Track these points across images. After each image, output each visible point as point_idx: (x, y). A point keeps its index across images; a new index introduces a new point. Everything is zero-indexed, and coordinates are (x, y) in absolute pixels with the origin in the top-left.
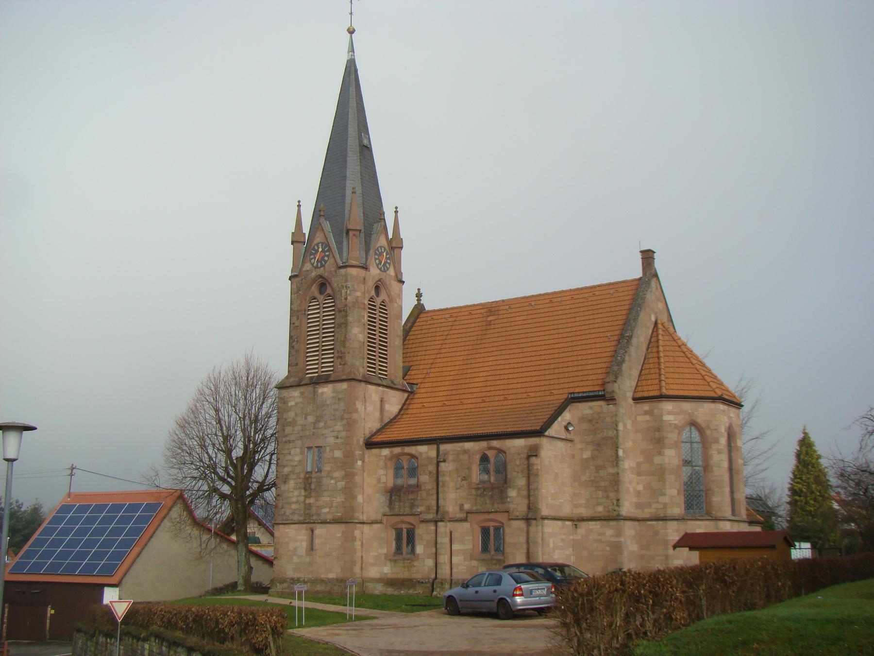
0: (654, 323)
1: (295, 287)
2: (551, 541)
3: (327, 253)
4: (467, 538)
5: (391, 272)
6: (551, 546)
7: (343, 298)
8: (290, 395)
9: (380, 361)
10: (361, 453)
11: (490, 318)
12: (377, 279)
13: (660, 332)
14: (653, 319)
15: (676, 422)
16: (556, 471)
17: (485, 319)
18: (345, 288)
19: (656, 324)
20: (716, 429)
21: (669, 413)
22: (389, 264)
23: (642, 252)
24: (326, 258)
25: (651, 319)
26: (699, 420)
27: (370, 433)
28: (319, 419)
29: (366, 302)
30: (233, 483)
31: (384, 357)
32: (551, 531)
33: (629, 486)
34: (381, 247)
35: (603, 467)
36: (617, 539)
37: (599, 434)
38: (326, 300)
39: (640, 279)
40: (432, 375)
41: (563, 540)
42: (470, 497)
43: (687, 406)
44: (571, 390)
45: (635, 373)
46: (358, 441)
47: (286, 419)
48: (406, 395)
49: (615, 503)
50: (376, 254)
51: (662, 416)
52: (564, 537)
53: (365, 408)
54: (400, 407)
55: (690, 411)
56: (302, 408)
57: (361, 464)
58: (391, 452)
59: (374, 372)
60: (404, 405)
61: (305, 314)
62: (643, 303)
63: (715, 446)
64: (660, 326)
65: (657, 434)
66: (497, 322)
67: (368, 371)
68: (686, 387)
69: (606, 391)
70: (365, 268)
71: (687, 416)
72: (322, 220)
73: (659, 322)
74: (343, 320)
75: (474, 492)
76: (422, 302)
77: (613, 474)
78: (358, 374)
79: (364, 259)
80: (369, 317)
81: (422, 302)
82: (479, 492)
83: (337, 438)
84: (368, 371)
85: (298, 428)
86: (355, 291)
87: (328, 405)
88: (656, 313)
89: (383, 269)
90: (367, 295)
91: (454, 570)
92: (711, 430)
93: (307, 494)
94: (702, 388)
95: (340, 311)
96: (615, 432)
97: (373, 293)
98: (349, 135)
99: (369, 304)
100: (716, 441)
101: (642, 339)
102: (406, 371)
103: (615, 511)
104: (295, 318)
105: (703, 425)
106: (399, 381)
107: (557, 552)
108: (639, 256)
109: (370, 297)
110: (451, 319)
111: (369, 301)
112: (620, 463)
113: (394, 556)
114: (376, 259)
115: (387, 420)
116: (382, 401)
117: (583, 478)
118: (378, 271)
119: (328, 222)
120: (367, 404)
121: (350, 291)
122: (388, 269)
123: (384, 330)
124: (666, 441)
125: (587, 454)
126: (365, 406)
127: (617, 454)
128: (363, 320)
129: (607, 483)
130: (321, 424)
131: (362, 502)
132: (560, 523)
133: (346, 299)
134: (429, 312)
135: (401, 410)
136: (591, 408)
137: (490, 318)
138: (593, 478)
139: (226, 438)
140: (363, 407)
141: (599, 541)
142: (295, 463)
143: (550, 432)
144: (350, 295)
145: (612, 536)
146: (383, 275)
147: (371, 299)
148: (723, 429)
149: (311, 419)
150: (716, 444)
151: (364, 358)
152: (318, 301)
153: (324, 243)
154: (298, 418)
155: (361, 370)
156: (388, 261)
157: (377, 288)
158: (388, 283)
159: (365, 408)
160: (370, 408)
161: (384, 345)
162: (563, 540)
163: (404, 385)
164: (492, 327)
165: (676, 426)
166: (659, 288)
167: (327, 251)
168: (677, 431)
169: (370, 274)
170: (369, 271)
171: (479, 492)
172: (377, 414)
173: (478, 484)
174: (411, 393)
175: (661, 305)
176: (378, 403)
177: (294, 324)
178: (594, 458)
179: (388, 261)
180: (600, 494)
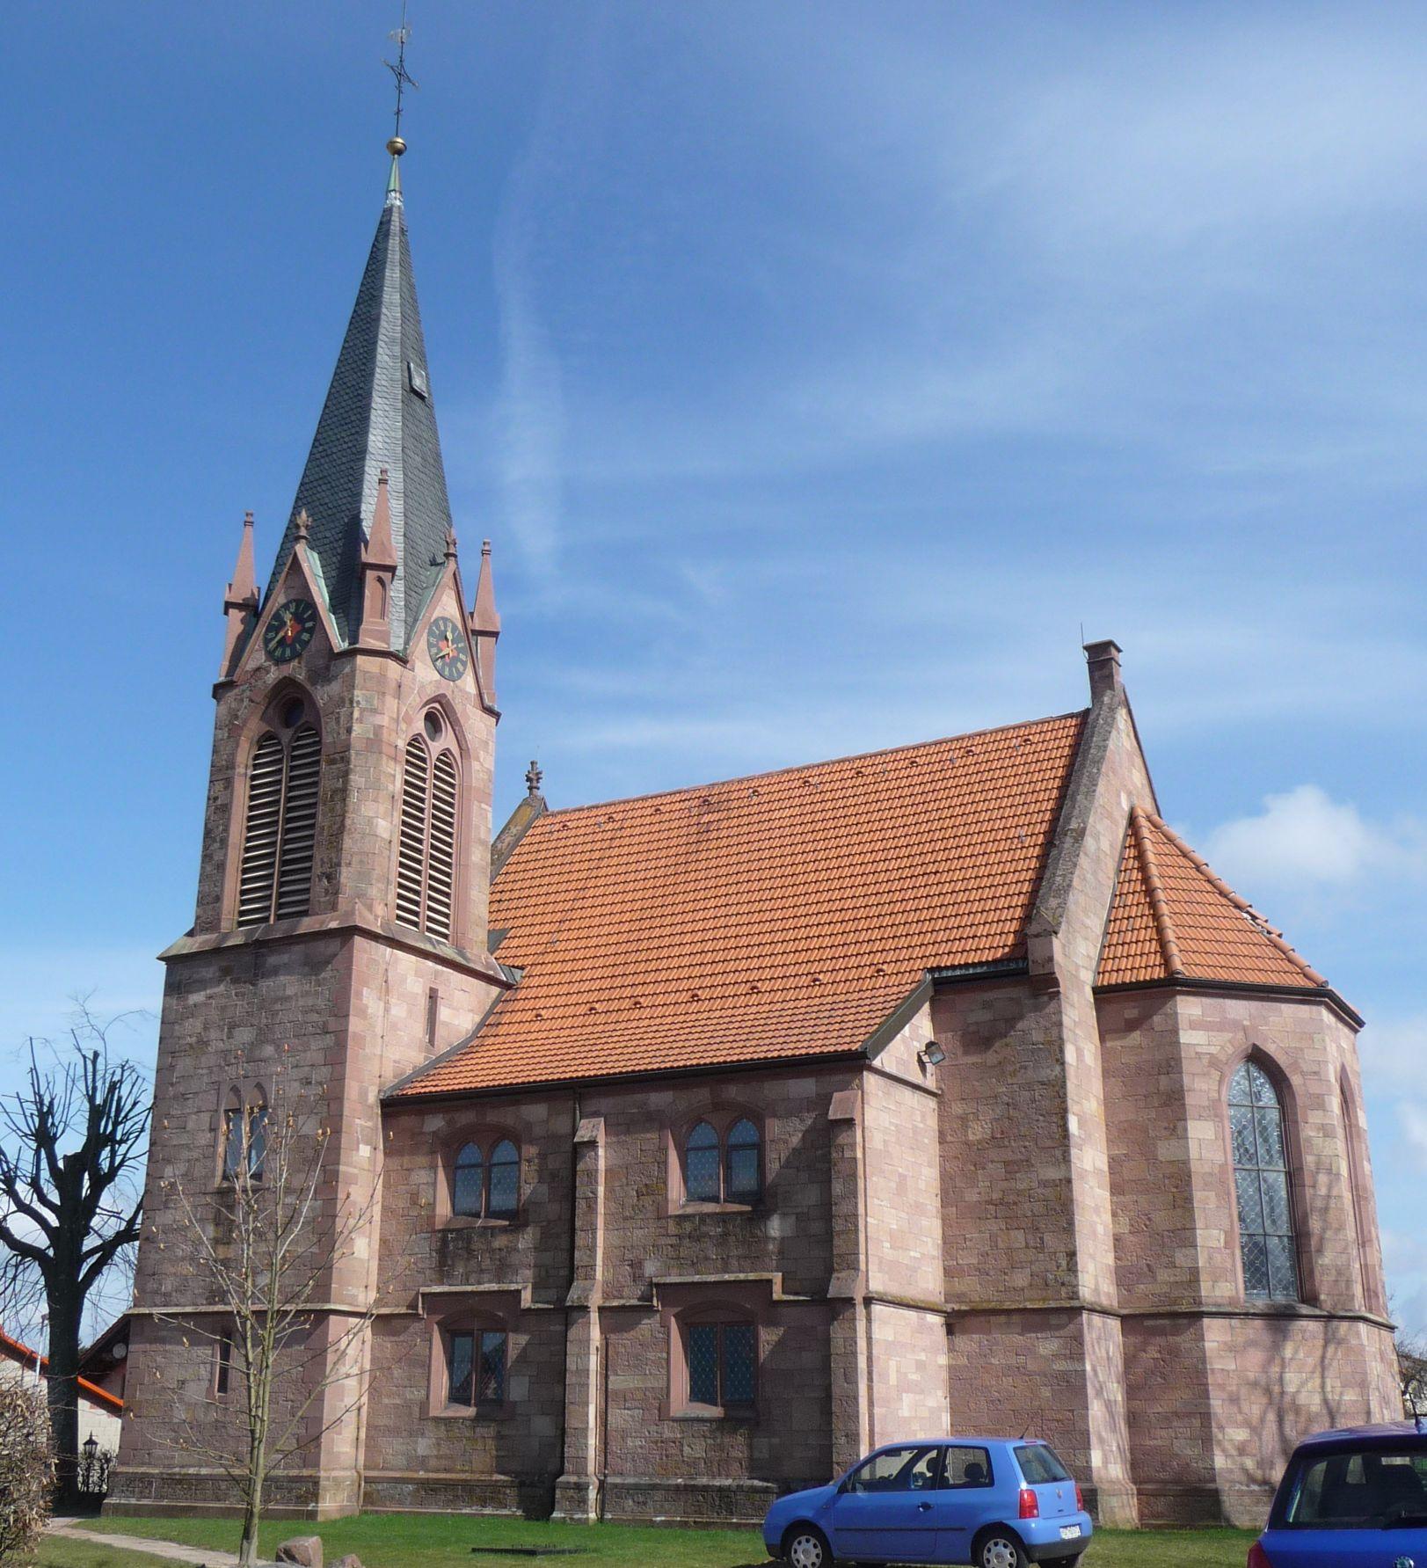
1: (223, 709)
2: (892, 1364)
3: (309, 624)
4: (651, 1355)
5: (468, 683)
6: (893, 1380)
9: (430, 909)
11: (706, 819)
12: (431, 692)
13: (1145, 832)
14: (1126, 807)
15: (1213, 1050)
17: (694, 820)
18: (347, 705)
19: (1132, 821)
21: (1194, 1026)
22: (464, 664)
23: (1086, 648)
24: (305, 636)
25: (1119, 803)
26: (1271, 1048)
27: (395, 1077)
28: (263, 1036)
29: (402, 744)
30: (53, 1220)
31: (442, 889)
33: (1095, 1218)
34: (445, 620)
38: (299, 739)
39: (1087, 712)
41: (920, 1366)
42: (663, 1241)
43: (1238, 1009)
44: (932, 962)
45: (1096, 924)
46: (363, 1094)
48: (495, 991)
49: (1064, 1263)
50: (431, 633)
51: (1175, 1032)
52: (923, 1357)
53: (387, 1010)
54: (478, 1019)
55: (1246, 1023)
56: (223, 1009)
58: (450, 1123)
59: (415, 924)
60: (490, 1013)
61: (246, 774)
62: (1103, 758)
63: (1315, 1117)
64: (1143, 822)
66: (725, 824)
67: (399, 918)
68: (1234, 962)
70: (402, 659)
71: (1240, 1035)
72: (301, 549)
73: (1140, 812)
74: (340, 784)
75: (672, 1228)
79: (402, 641)
80: (407, 783)
81: (538, 793)
82: (688, 1227)
84: (399, 918)
85: (210, 1060)
86: (374, 711)
87: (288, 999)
88: (1129, 794)
89: (447, 673)
90: (403, 726)
91: (614, 1447)
93: (220, 1235)
94: (1272, 965)
95: (332, 762)
96: (1058, 1068)
97: (419, 726)
98: (378, 363)
99: (409, 753)
100: (1319, 1103)
101: (1105, 845)
102: (496, 939)
103: (1063, 1284)
104: (219, 786)
106: (479, 956)
108: (1083, 657)
111: (410, 744)
112: (1074, 1152)
113: (446, 1408)
114: (430, 645)
115: (442, 1047)
116: (433, 996)
117: (972, 1196)
118: (437, 676)
119: (316, 555)
120: (393, 1001)
121: (362, 711)
122: (460, 675)
123: (444, 822)
124: (1190, 1100)
125: (977, 1132)
126: (387, 1003)
128: (391, 787)
129: (1038, 1208)
130: (269, 1050)
132: (912, 1315)
133: (349, 731)
134: (554, 815)
135: (482, 1024)
136: (987, 1005)
137: (706, 819)
139: (45, 1113)
140: (382, 1004)
141: (1020, 1370)
142: (195, 1155)
143: (885, 1060)
144: (360, 720)
146: (447, 688)
147: (415, 741)
148: (1332, 1075)
149: (245, 1035)
150: (1320, 1113)
152: (279, 743)
153: (302, 601)
154: (213, 1034)
155: (380, 910)
156: (461, 656)
157: (432, 720)
158: (458, 708)
159: (387, 1010)
160: (398, 1011)
161: (444, 859)
162: (920, 1366)
163: (488, 966)
165: (1214, 1062)
168: (1216, 1075)
169: (414, 678)
170: (413, 670)
171: (688, 1227)
172: (419, 1029)
173: (684, 1206)
174: (507, 986)
175: (1138, 778)
176: (423, 1003)
177: (216, 799)
179: (461, 656)
180: (1019, 1238)
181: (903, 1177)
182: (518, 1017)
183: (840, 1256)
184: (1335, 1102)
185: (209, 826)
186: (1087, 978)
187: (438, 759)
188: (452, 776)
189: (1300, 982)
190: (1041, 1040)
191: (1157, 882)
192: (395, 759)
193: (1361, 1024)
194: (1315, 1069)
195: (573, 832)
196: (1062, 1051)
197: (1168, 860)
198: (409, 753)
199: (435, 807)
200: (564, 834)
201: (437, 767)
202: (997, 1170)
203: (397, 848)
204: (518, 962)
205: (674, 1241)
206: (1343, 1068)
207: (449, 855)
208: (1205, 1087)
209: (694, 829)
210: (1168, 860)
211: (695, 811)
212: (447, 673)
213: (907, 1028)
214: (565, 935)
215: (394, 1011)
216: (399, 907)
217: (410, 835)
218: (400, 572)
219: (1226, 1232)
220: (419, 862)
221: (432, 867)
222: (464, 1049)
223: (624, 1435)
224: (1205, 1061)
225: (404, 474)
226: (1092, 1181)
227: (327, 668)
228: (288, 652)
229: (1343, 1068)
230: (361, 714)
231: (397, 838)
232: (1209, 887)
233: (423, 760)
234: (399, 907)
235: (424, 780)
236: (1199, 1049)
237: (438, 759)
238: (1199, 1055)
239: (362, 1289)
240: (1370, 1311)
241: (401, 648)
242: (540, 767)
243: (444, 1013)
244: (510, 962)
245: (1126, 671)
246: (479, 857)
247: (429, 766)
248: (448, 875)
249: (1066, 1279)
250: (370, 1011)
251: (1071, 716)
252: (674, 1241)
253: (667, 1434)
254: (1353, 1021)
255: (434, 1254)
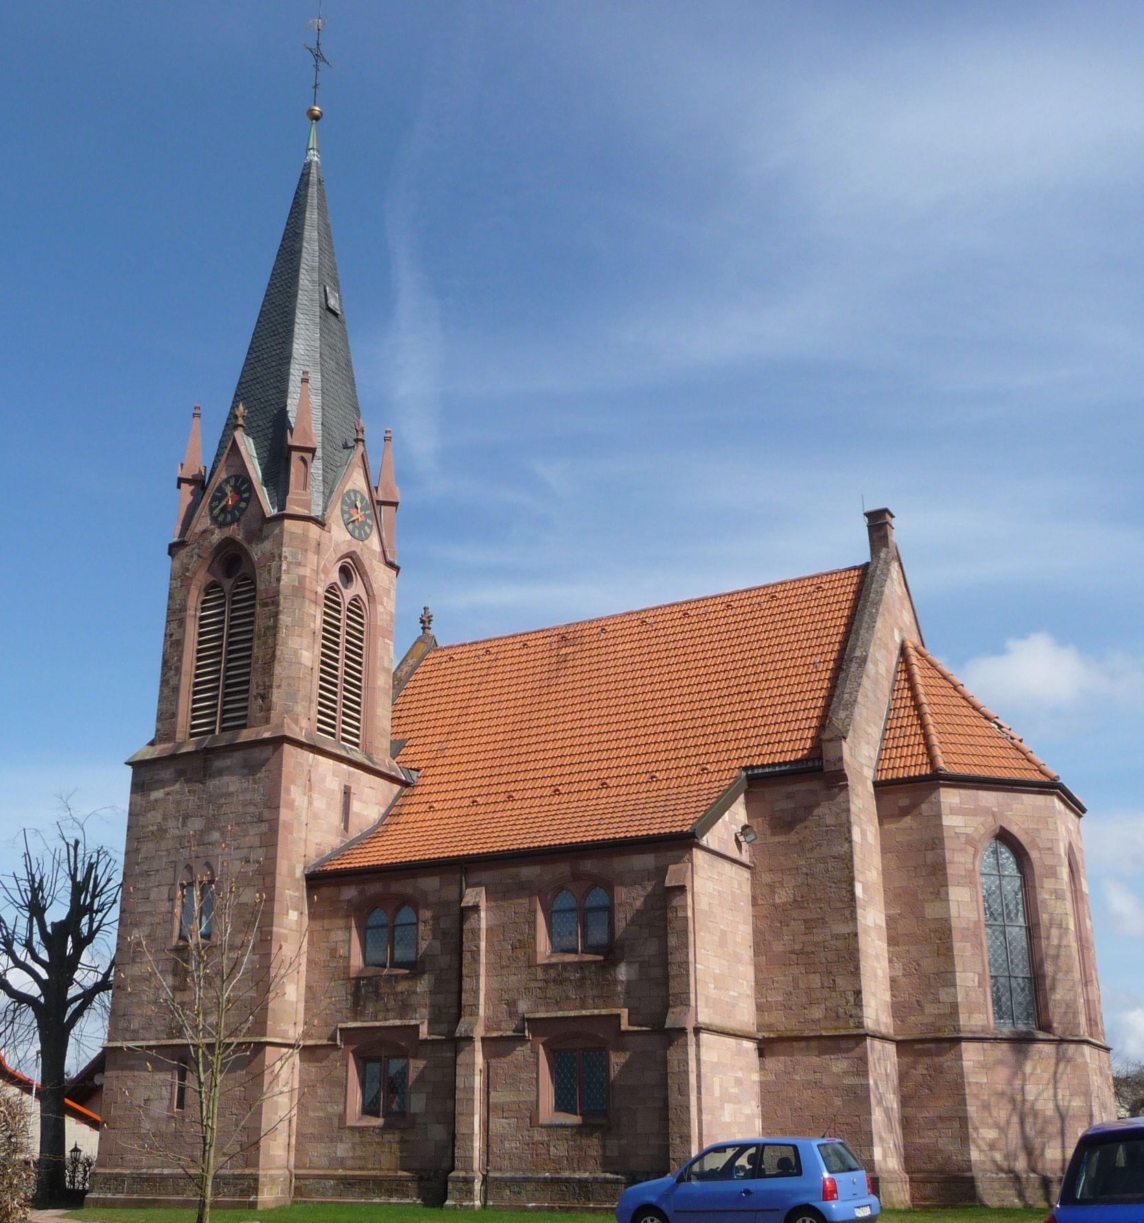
0: (898, 646)
1: (177, 563)
2: (717, 1080)
3: (245, 495)
4: (524, 1075)
5: (374, 543)
6: (717, 1093)
7: (273, 580)
8: (156, 777)
9: (344, 722)
10: (297, 894)
11: (563, 651)
12: (344, 549)
13: (914, 660)
14: (898, 640)
15: (969, 831)
16: (722, 927)
17: (554, 653)
18: (277, 559)
19: (903, 651)
20: (1049, 849)
21: (954, 811)
22: (371, 527)
23: (868, 515)
24: (243, 505)
25: (893, 637)
26: (1014, 830)
27: (316, 857)
29: (321, 591)
30: (44, 975)
31: (354, 707)
32: (715, 1060)
33: (876, 964)
34: (355, 492)
35: (822, 921)
36: (856, 1081)
37: (812, 849)
38: (238, 587)
39: (867, 565)
40: (447, 753)
41: (738, 1082)
42: (533, 985)
43: (989, 798)
44: (746, 762)
45: (876, 732)
47: (143, 827)
48: (397, 788)
49: (852, 999)
50: (344, 502)
51: (939, 816)
52: (740, 1074)
53: (310, 803)
54: (383, 810)
55: (995, 809)
56: (178, 803)
57: (295, 918)
59: (333, 735)
60: (392, 806)
61: (195, 616)
62: (880, 601)
63: (1048, 884)
64: (911, 651)
65: (930, 856)
66: (579, 655)
67: (320, 730)
68: (984, 761)
69: (825, 758)
70: (321, 523)
71: (990, 819)
72: (239, 435)
73: (909, 644)
74: (271, 623)
75: (540, 974)
76: (430, 632)
77: (844, 937)
78: (297, 729)
81: (430, 632)
82: (553, 973)
83: (248, 861)
84: (320, 730)
85: (167, 844)
86: (299, 564)
88: (901, 630)
90: (322, 576)
91: (495, 1148)
92: (1040, 850)
93: (177, 984)
94: (1015, 764)
95: (265, 605)
96: (847, 845)
97: (335, 576)
98: (300, 287)
99: (326, 598)
100: (1053, 873)
101: (882, 670)
102: (397, 748)
103: (851, 1016)
104: (174, 625)
105: (1023, 838)
106: (384, 762)
107: (728, 1107)
108: (863, 523)
109: (328, 583)
110: (487, 658)
111: (327, 591)
112: (859, 911)
113: (360, 1119)
114: (343, 512)
115: (354, 833)
116: (347, 792)
117: (778, 947)
118: (349, 537)
119: (251, 440)
120: (315, 795)
121: (289, 564)
122: (367, 536)
123: (355, 653)
124: (950, 870)
125: (782, 897)
126: (310, 797)
127: (852, 893)
128: (312, 625)
129: (832, 956)
130: (216, 836)
131: (295, 1000)
132: (732, 1042)
133: (279, 580)
134: (442, 649)
135: (387, 814)
136: (790, 796)
137: (563, 651)
138: (797, 947)
140: (306, 798)
141: (817, 1084)
143: (709, 840)
144: (288, 572)
145: (846, 1073)
146: (357, 547)
147: (331, 589)
148: (1062, 851)
149: (196, 824)
150: (1053, 880)
151: (311, 702)
152: (222, 591)
154: (171, 823)
155: (304, 723)
157: (345, 573)
158: (366, 563)
159: (310, 803)
160: (319, 804)
161: (355, 683)
162: (738, 1082)
164: (570, 664)
165: (970, 840)
166: (902, 583)
167: (244, 492)
168: (971, 850)
169: (331, 538)
170: (329, 532)
171: (553, 973)
172: (336, 818)
173: (549, 957)
174: (406, 784)
175: (907, 617)
176: (339, 797)
177: (171, 635)
178: (797, 903)
180: (816, 980)
181: (723, 933)
182: (415, 809)
183: (674, 995)
184: (1064, 872)
185: (166, 657)
186: (869, 774)
187: (350, 603)
188: (361, 617)
189: (1038, 777)
190: (833, 823)
191: (923, 699)
192: (316, 603)
193: (1084, 811)
194: (1049, 845)
195: (458, 663)
196: (850, 832)
197: (931, 682)
198: (326, 598)
199: (348, 641)
200: (451, 664)
201: (349, 610)
202: (798, 926)
203: (317, 674)
204: (415, 766)
205: (541, 984)
206: (1070, 845)
207: (359, 680)
208: (962, 860)
209: (554, 660)
210: (931, 682)
211: (555, 645)
212: (357, 534)
213: (727, 813)
214: (452, 744)
215: (316, 804)
216: (320, 721)
217: (328, 664)
218: (319, 453)
219: (979, 974)
220: (335, 685)
221: (346, 689)
222: (373, 834)
223: (503, 1138)
224: (963, 839)
225: (322, 375)
226: (874, 935)
227: (261, 530)
228: (229, 516)
229: (1070, 845)
230: (288, 566)
231: (318, 666)
232: (965, 703)
233: (338, 604)
234: (320, 721)
235: (339, 620)
236: (957, 830)
237: (350, 603)
238: (957, 835)
239: (292, 1025)
240: (1091, 1035)
241: (320, 514)
242: (431, 612)
243: (356, 806)
244: (408, 765)
245: (899, 533)
246: (383, 681)
247: (343, 609)
248: (358, 696)
249: (853, 1012)
250: (296, 804)
251: (855, 568)
252: (541, 984)
253: (537, 1138)
254: (1078, 809)
255: (349, 997)
